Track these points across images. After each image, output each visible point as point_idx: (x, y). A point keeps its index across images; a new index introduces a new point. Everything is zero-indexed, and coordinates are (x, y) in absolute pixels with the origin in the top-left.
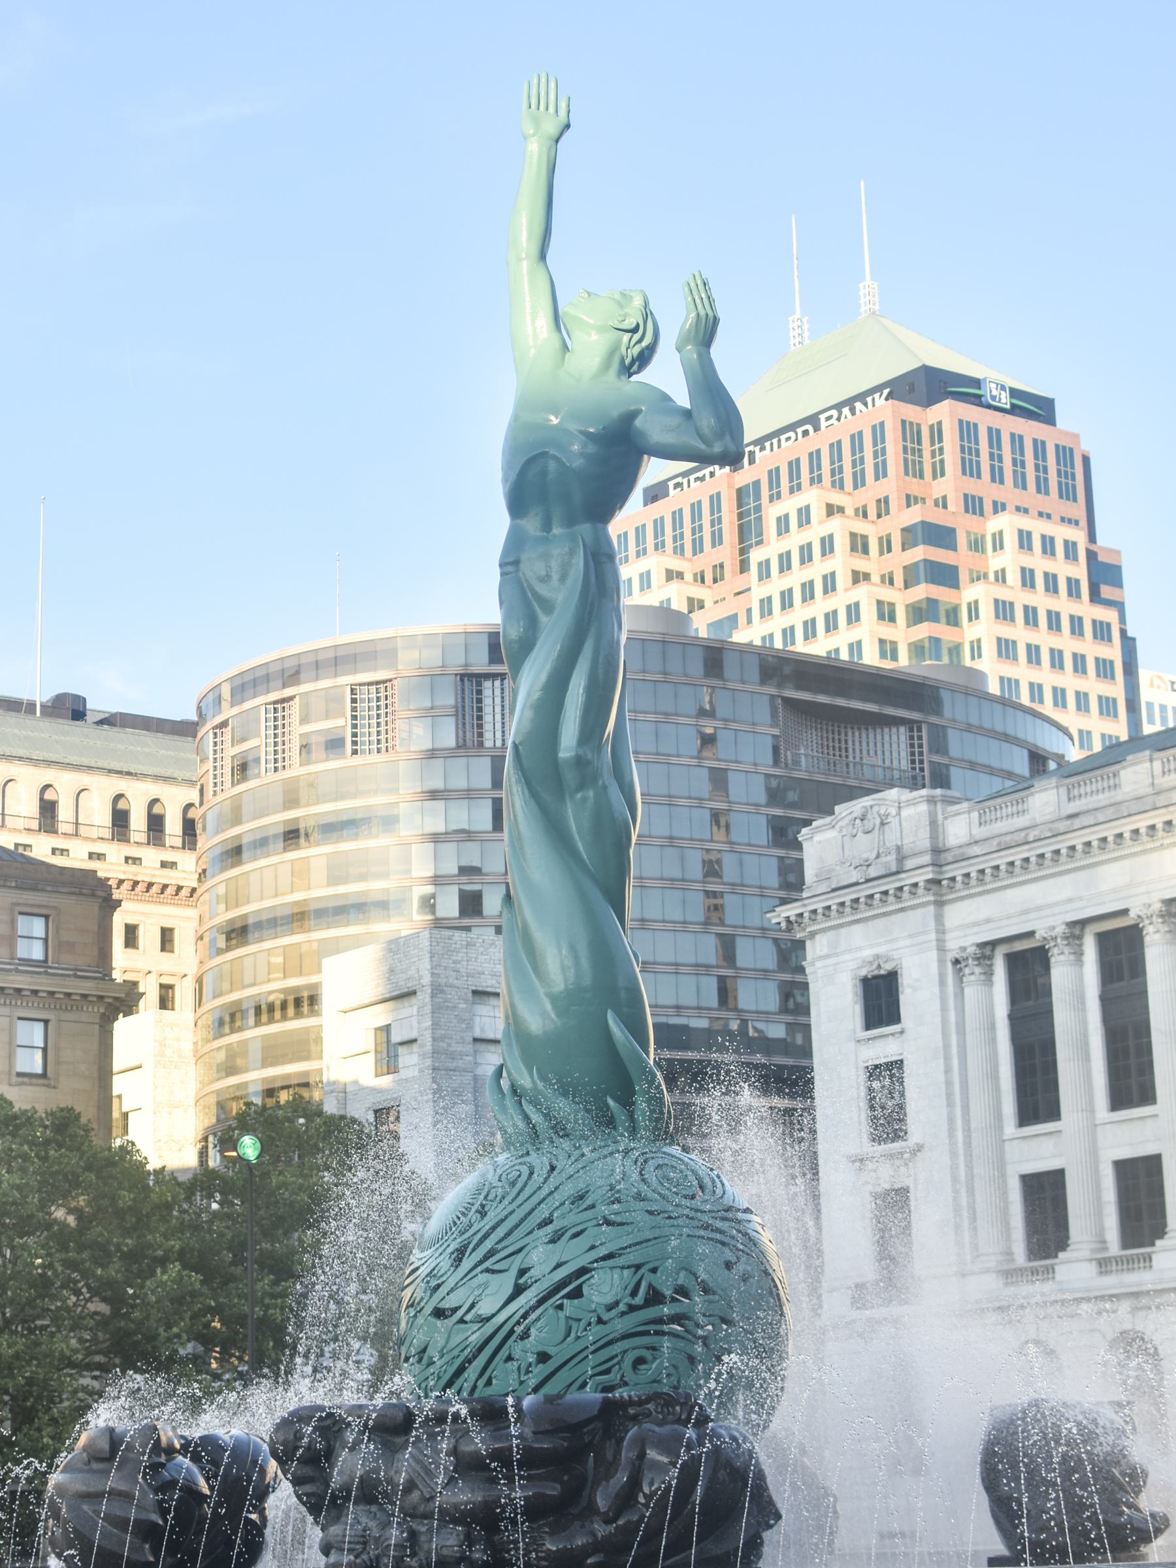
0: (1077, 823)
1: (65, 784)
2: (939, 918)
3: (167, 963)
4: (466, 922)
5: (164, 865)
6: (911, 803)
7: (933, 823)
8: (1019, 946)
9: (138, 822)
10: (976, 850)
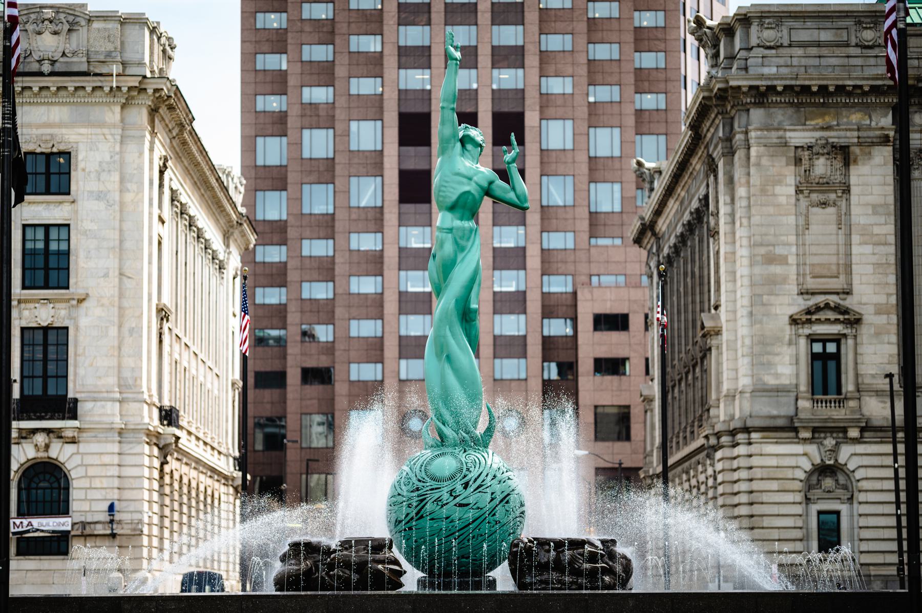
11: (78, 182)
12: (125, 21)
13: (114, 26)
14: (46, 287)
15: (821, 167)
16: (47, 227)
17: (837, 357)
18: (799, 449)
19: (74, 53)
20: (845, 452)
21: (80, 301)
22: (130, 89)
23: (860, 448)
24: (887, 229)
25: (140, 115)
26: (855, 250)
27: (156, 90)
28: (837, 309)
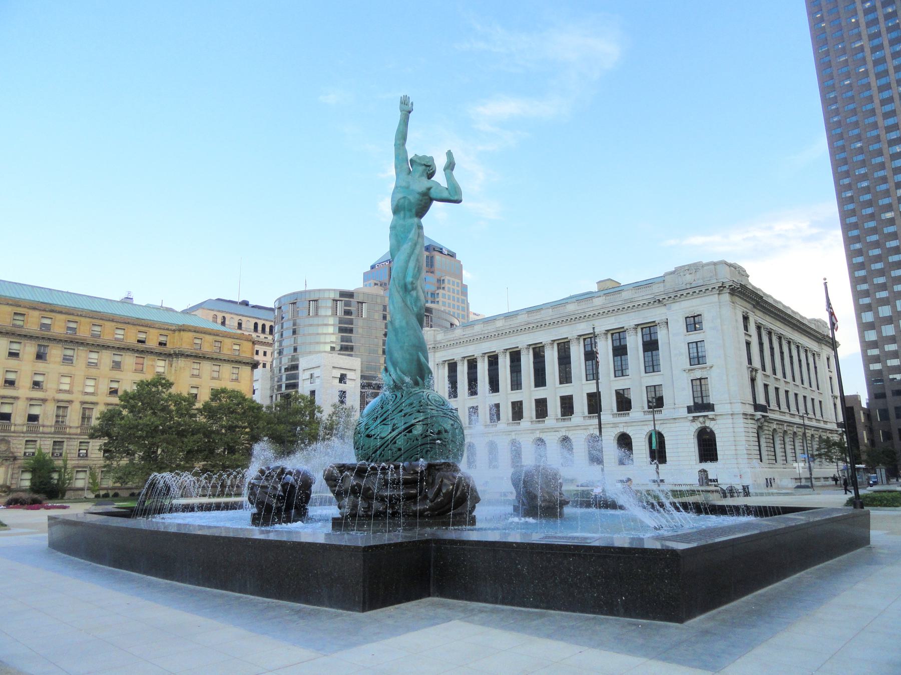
0: (465, 336)
1: (244, 319)
2: (434, 355)
3: (265, 359)
4: (332, 352)
5: (265, 338)
6: (429, 331)
7: (434, 336)
8: (451, 362)
9: (260, 328)
10: (443, 341)
11: (705, 325)
12: (715, 264)
13: (712, 267)
14: (699, 364)
16: (696, 342)
19: (698, 279)
21: (711, 367)
22: (719, 287)
25: (726, 297)
27: (730, 286)
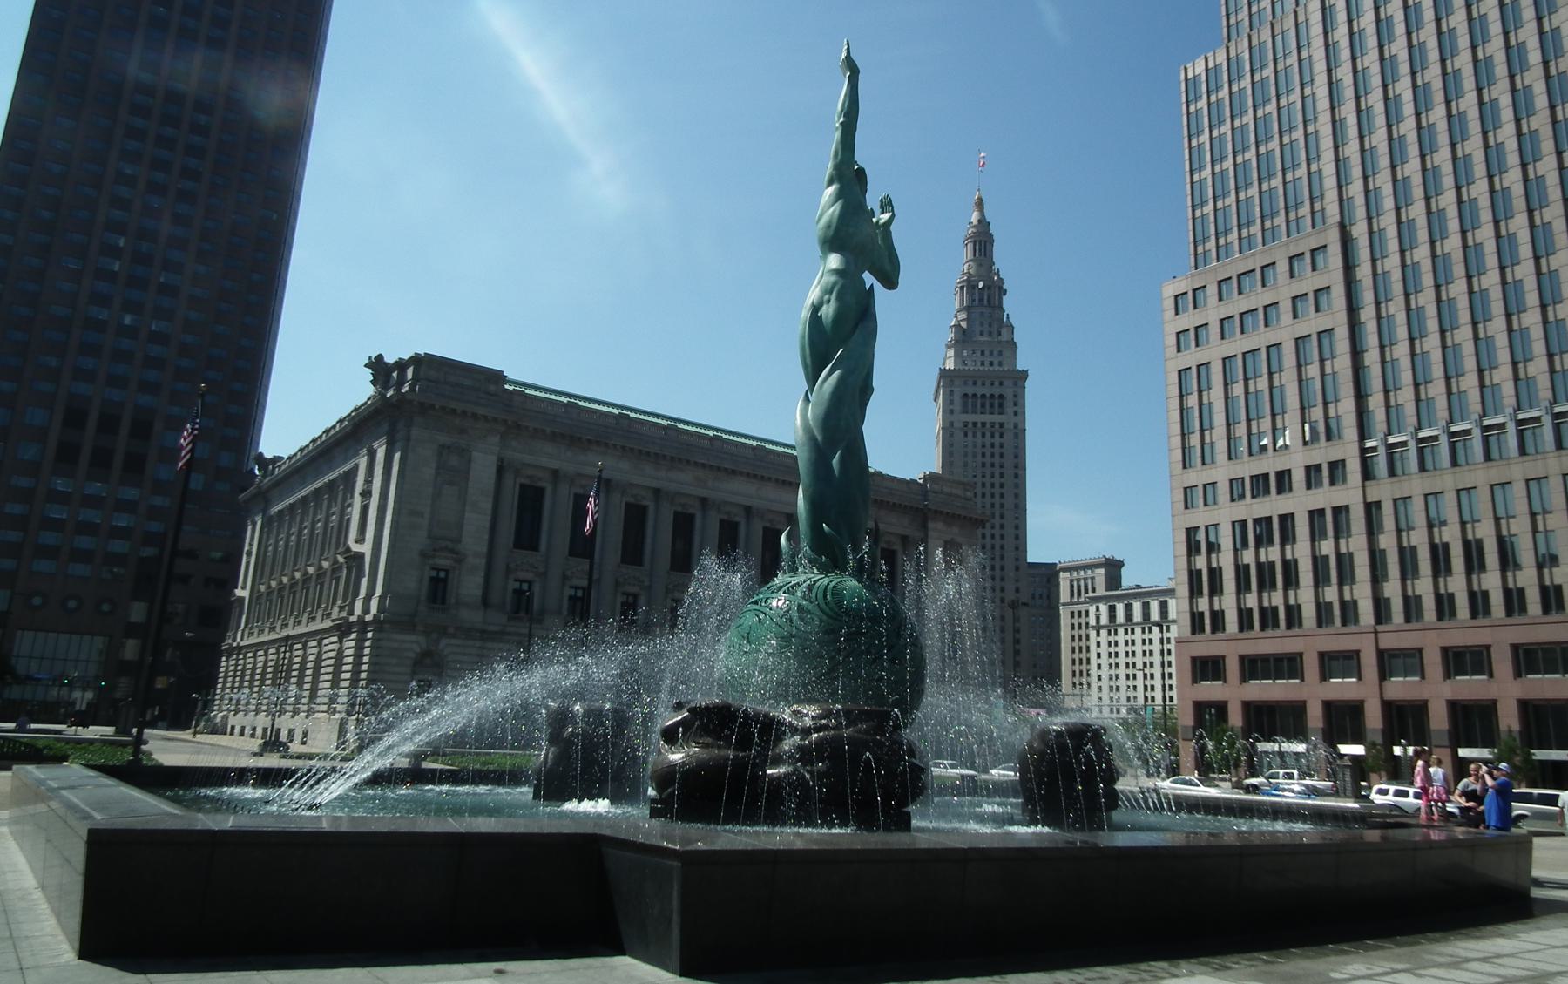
15: (454, 460)
17: (445, 581)
18: (413, 638)
20: (444, 642)
23: (454, 641)
24: (488, 505)
26: (467, 515)
28: (452, 551)
